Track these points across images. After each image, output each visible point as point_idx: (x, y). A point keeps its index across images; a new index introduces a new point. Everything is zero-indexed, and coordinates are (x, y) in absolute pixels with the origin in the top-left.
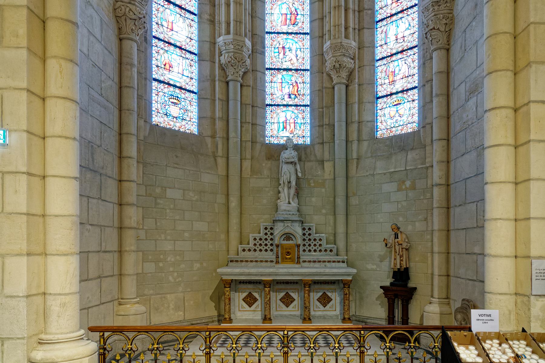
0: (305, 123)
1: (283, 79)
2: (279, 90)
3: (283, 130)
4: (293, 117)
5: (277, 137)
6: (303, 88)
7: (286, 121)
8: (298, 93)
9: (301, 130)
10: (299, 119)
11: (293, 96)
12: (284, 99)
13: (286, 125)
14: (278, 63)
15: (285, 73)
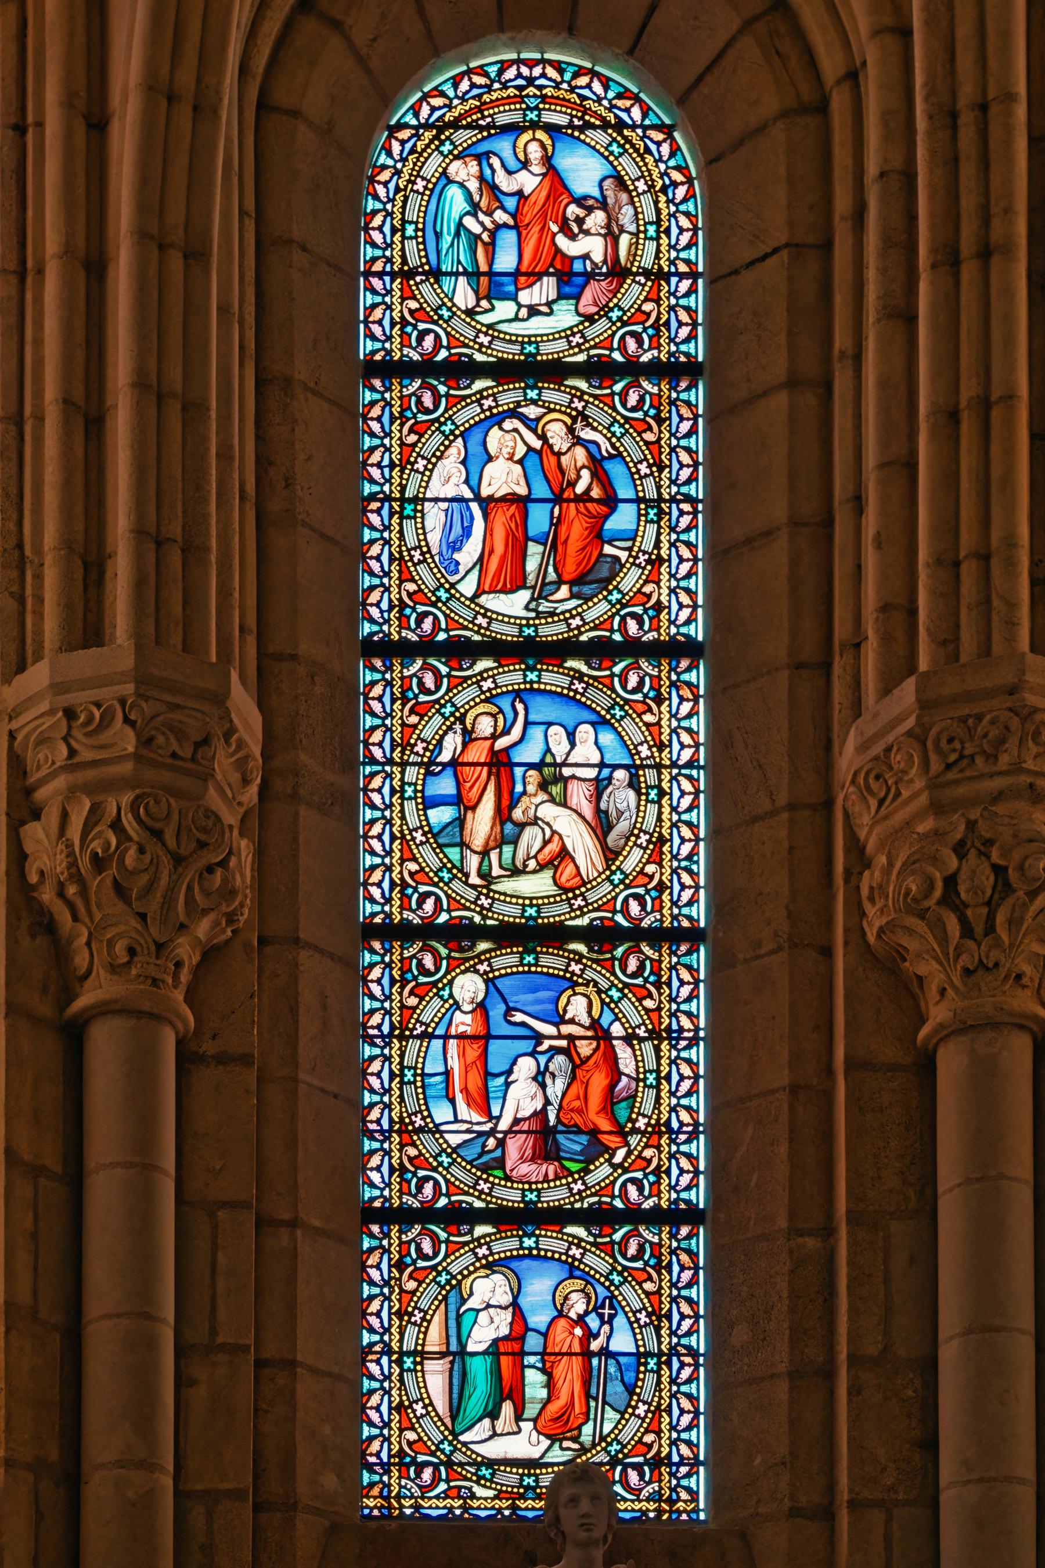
0: (673, 1351)
1: (497, 1011)
2: (459, 1098)
3: (493, 1415)
4: (578, 1306)
5: (449, 1464)
6: (651, 1079)
7: (522, 1339)
8: (613, 1119)
9: (642, 1409)
10: (620, 1321)
11: (572, 1144)
12: (501, 1163)
13: (520, 1369)
14: (456, 885)
15: (506, 960)
